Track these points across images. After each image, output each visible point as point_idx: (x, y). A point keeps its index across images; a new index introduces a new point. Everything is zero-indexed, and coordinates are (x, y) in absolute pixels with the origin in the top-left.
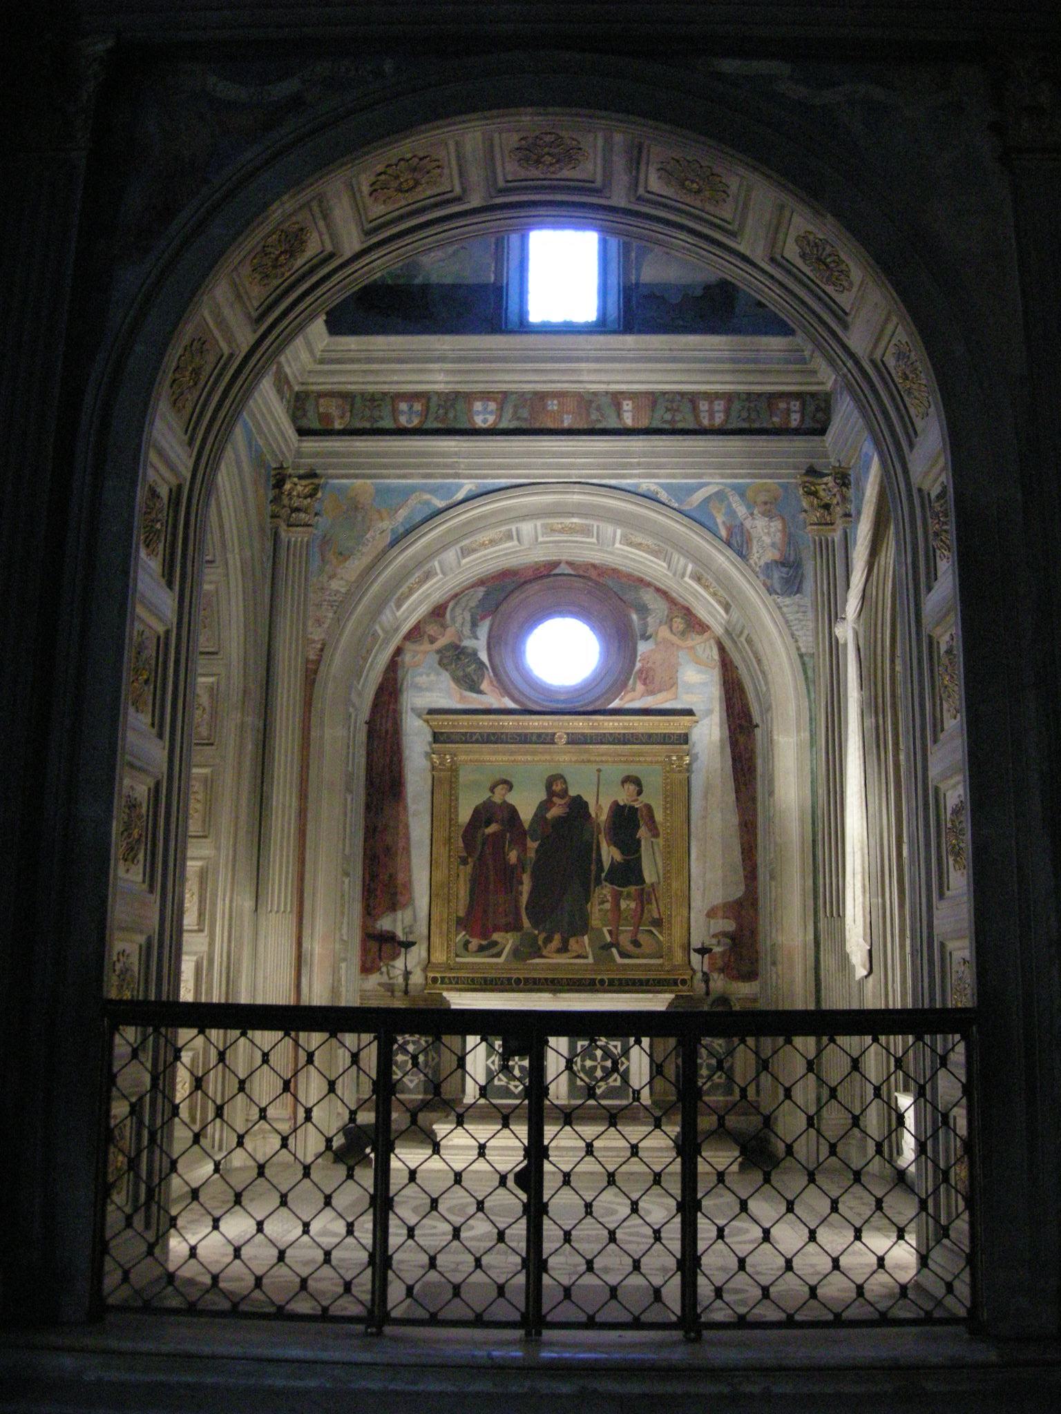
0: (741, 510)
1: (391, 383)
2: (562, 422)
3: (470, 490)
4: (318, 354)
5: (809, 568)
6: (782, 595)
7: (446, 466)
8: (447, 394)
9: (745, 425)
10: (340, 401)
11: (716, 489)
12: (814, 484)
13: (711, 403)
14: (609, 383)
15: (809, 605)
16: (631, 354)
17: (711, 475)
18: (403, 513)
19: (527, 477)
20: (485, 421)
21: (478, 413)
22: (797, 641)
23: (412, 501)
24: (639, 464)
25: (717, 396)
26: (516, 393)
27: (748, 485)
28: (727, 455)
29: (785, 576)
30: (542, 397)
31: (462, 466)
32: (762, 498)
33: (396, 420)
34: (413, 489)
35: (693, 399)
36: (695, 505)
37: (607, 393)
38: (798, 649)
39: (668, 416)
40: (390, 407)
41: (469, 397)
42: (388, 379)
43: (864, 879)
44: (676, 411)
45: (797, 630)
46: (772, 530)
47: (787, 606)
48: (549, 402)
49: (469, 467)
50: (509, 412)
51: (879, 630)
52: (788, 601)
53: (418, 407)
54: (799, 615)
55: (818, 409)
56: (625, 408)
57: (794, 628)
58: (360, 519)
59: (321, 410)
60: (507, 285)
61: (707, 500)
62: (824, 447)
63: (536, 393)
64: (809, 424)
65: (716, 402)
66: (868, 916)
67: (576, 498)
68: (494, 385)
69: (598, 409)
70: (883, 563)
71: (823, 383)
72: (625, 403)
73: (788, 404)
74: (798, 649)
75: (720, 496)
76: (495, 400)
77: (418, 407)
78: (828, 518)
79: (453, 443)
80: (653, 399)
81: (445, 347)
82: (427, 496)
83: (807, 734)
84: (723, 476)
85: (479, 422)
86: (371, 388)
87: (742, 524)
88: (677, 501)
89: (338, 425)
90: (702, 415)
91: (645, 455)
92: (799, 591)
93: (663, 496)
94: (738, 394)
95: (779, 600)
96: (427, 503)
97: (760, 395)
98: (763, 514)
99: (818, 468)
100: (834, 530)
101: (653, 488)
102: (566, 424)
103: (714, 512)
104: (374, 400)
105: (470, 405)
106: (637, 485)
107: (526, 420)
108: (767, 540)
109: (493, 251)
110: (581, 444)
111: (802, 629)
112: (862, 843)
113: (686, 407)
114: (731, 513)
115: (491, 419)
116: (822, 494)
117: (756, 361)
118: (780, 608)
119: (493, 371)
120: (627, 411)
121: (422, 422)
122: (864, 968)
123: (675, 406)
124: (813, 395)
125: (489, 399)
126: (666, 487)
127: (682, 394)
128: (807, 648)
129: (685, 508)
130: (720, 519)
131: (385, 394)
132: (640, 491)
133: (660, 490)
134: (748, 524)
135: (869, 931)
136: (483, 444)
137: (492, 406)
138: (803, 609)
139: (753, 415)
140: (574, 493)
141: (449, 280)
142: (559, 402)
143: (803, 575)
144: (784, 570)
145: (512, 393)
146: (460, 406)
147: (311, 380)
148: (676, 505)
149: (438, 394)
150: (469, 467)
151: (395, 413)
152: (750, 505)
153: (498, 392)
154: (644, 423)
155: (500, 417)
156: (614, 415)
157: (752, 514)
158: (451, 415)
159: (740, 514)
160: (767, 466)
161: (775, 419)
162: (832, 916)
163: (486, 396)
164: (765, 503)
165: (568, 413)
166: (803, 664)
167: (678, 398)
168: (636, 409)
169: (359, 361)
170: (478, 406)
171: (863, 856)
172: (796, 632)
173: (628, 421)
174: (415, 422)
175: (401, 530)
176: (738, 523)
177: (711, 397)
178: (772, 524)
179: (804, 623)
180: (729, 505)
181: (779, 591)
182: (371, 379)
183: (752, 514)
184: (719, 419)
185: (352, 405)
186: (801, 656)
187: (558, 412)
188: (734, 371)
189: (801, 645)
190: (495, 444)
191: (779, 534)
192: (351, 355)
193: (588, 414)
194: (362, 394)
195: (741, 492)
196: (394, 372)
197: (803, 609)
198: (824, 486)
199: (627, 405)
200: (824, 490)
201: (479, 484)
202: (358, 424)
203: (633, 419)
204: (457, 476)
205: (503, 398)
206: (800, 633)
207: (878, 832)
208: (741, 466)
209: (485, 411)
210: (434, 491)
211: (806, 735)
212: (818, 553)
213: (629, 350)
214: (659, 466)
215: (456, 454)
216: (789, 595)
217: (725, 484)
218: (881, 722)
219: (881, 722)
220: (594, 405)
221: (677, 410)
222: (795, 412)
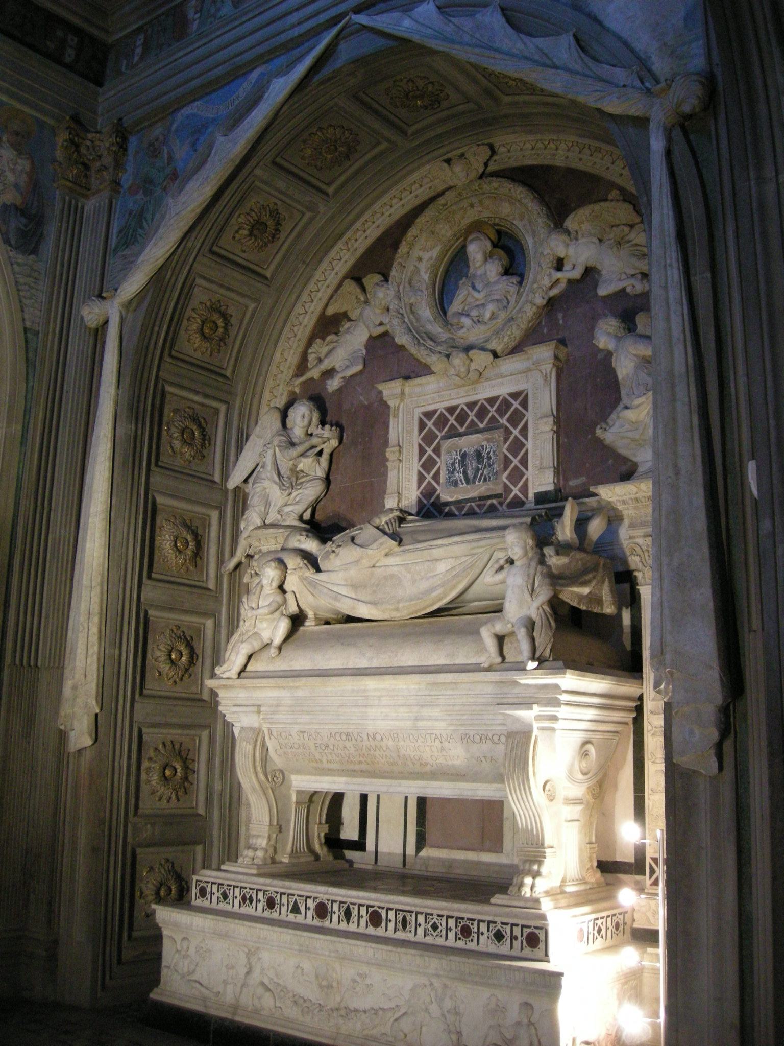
5: (51, 231)
6: (16, 249)
12: (78, 135)
15: (43, 272)
22: (23, 311)
29: (22, 227)
38: (24, 320)
43: (101, 622)
45: (24, 297)
46: (19, 168)
47: (19, 264)
51: (158, 323)
52: (21, 258)
54: (30, 280)
57: (22, 294)
66: (101, 670)
70: (190, 244)
71: (107, 32)
74: (24, 320)
83: (20, 427)
92: (34, 251)
95: (11, 254)
98: (13, 145)
100: (86, 197)
108: (11, 178)
111: (31, 298)
112: (103, 577)
116: (83, 150)
118: (12, 265)
122: (90, 736)
128: (33, 322)
135: (100, 690)
138: (36, 275)
143: (42, 234)
144: (24, 220)
161: (48, 43)
162: (22, 665)
166: (26, 341)
171: (102, 593)
172: (24, 301)
178: (19, 161)
179: (33, 291)
181: (13, 242)
186: (26, 330)
189: (26, 316)
191: (24, 177)
197: (36, 275)
198: (88, 143)
200: (88, 147)
206: (27, 302)
207: (123, 567)
211: (17, 428)
212: (65, 219)
216: (24, 253)
218: (139, 432)
219: (139, 432)
222: (71, 47)
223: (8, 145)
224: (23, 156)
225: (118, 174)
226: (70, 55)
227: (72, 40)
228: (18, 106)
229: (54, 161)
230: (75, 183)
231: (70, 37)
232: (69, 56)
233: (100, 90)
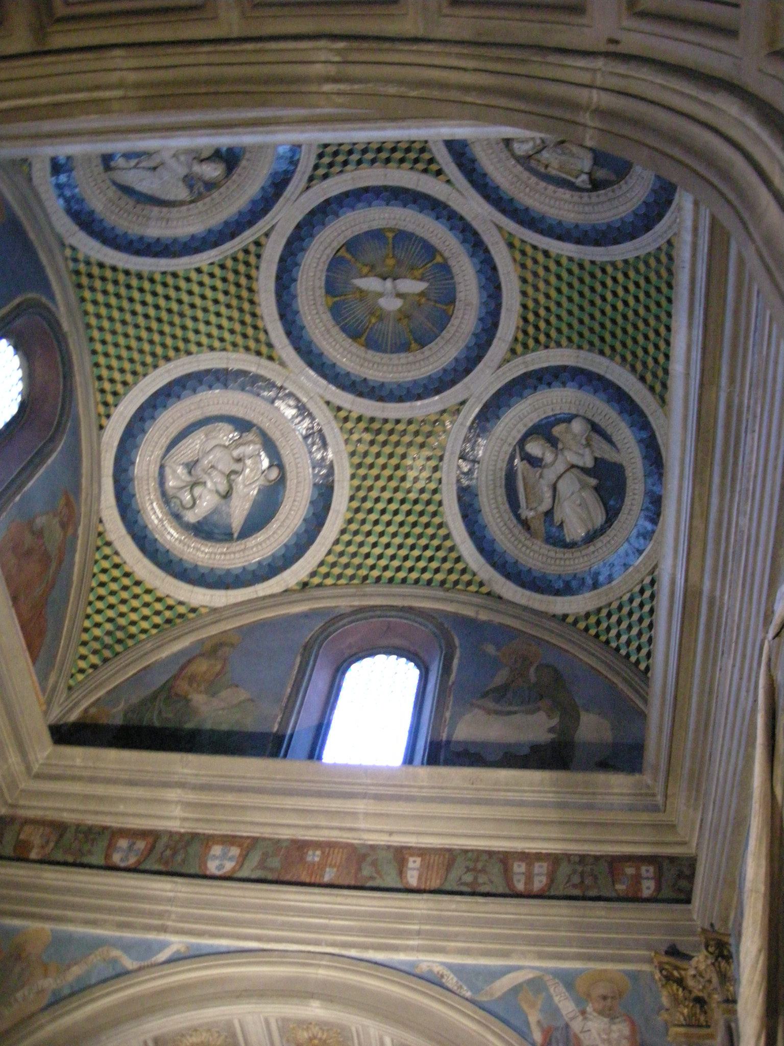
0: (567, 1006)
1: (116, 814)
2: (322, 876)
3: (178, 952)
4: (36, 768)
7: (151, 914)
8: (182, 835)
9: (576, 892)
10: (48, 830)
11: (531, 976)
12: (677, 968)
13: (530, 865)
14: (391, 833)
16: (425, 793)
17: (524, 954)
18: (76, 971)
19: (258, 939)
20: (220, 867)
21: (215, 857)
23: (95, 958)
24: (419, 933)
25: (539, 857)
26: (270, 839)
27: (578, 973)
28: (546, 926)
30: (301, 846)
31: (173, 917)
32: (601, 990)
33: (108, 856)
34: (100, 943)
35: (505, 859)
36: (498, 994)
37: (389, 847)
39: (468, 878)
40: (105, 843)
41: (208, 840)
42: (113, 810)
44: (480, 871)
46: (615, 1035)
48: (310, 853)
49: (183, 918)
50: (255, 858)
53: (141, 845)
55: (680, 875)
56: (411, 864)
58: (17, 969)
59: (22, 837)
60: (292, 736)
61: (516, 990)
62: (691, 920)
63: (294, 842)
64: (666, 893)
65: (537, 865)
67: (322, 973)
68: (242, 827)
69: (374, 864)
71: (684, 843)
72: (411, 859)
73: (638, 869)
75: (536, 985)
76: (240, 846)
77: (141, 845)
78: (702, 1018)
79: (168, 886)
80: (450, 857)
81: (186, 771)
82: (116, 953)
84: (541, 956)
85: (212, 867)
86: (91, 820)
87: (567, 1026)
88: (471, 988)
89: (33, 855)
90: (515, 878)
91: (427, 919)
93: (451, 980)
94: (567, 856)
96: (115, 961)
97: (597, 858)
98: (601, 1013)
99: (682, 949)
101: (437, 969)
102: (327, 879)
103: (525, 1007)
104: (91, 834)
105: (208, 848)
106: (414, 964)
107: (271, 870)
109: (283, 704)
110: (339, 900)
113: (496, 869)
114: (553, 1011)
115: (229, 866)
116: (691, 983)
117: (590, 807)
119: (244, 808)
120: (414, 869)
121: (139, 862)
123: (480, 866)
124: (672, 859)
125: (232, 844)
126: (458, 970)
127: (490, 854)
129: (483, 998)
130: (533, 1018)
131: (105, 828)
132: (417, 971)
133: (446, 972)
134: (576, 1026)
136: (208, 890)
137: (235, 851)
139: (588, 881)
140: (319, 966)
141: (224, 727)
142: (323, 853)
145: (264, 839)
146: (194, 848)
147: (22, 802)
148: (468, 994)
149: (171, 834)
150: (183, 918)
151: (111, 847)
152: (581, 1001)
153: (248, 837)
154: (435, 884)
155: (241, 864)
156: (393, 873)
157: (583, 1013)
158: (179, 858)
159: (564, 1012)
160: (607, 943)
163: (229, 840)
164: (605, 998)
165: (331, 866)
167: (485, 857)
168: (426, 867)
169: (79, 779)
170: (217, 850)
173: (413, 880)
174: (132, 861)
175: (67, 991)
176: (560, 1024)
177: (527, 857)
178: (614, 1027)
180: (550, 998)
182: (92, 807)
183: (583, 1013)
184: (539, 883)
185: (61, 836)
187: (319, 863)
188: (562, 823)
190: (222, 892)
192: (77, 772)
193: (359, 869)
194: (78, 826)
195: (568, 980)
196: (122, 799)
199: (414, 863)
201: (192, 945)
202: (60, 857)
203: (420, 878)
204: (164, 929)
205: (248, 845)
208: (569, 942)
209: (224, 856)
210: (127, 947)
213: (421, 787)
214: (447, 937)
215: (170, 901)
217: (546, 970)
220: (369, 859)
221: (483, 871)
222: (647, 878)
223: (595, 1014)
224: (617, 1020)
225: (728, 990)
226: (648, 888)
227: (647, 871)
228: (592, 965)
229: (661, 1008)
230: (689, 1025)
231: (644, 869)
232: (648, 888)
233: (690, 907)
